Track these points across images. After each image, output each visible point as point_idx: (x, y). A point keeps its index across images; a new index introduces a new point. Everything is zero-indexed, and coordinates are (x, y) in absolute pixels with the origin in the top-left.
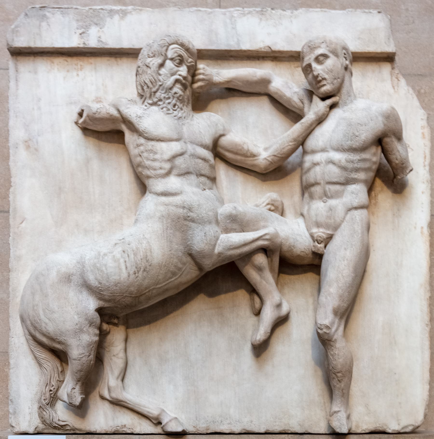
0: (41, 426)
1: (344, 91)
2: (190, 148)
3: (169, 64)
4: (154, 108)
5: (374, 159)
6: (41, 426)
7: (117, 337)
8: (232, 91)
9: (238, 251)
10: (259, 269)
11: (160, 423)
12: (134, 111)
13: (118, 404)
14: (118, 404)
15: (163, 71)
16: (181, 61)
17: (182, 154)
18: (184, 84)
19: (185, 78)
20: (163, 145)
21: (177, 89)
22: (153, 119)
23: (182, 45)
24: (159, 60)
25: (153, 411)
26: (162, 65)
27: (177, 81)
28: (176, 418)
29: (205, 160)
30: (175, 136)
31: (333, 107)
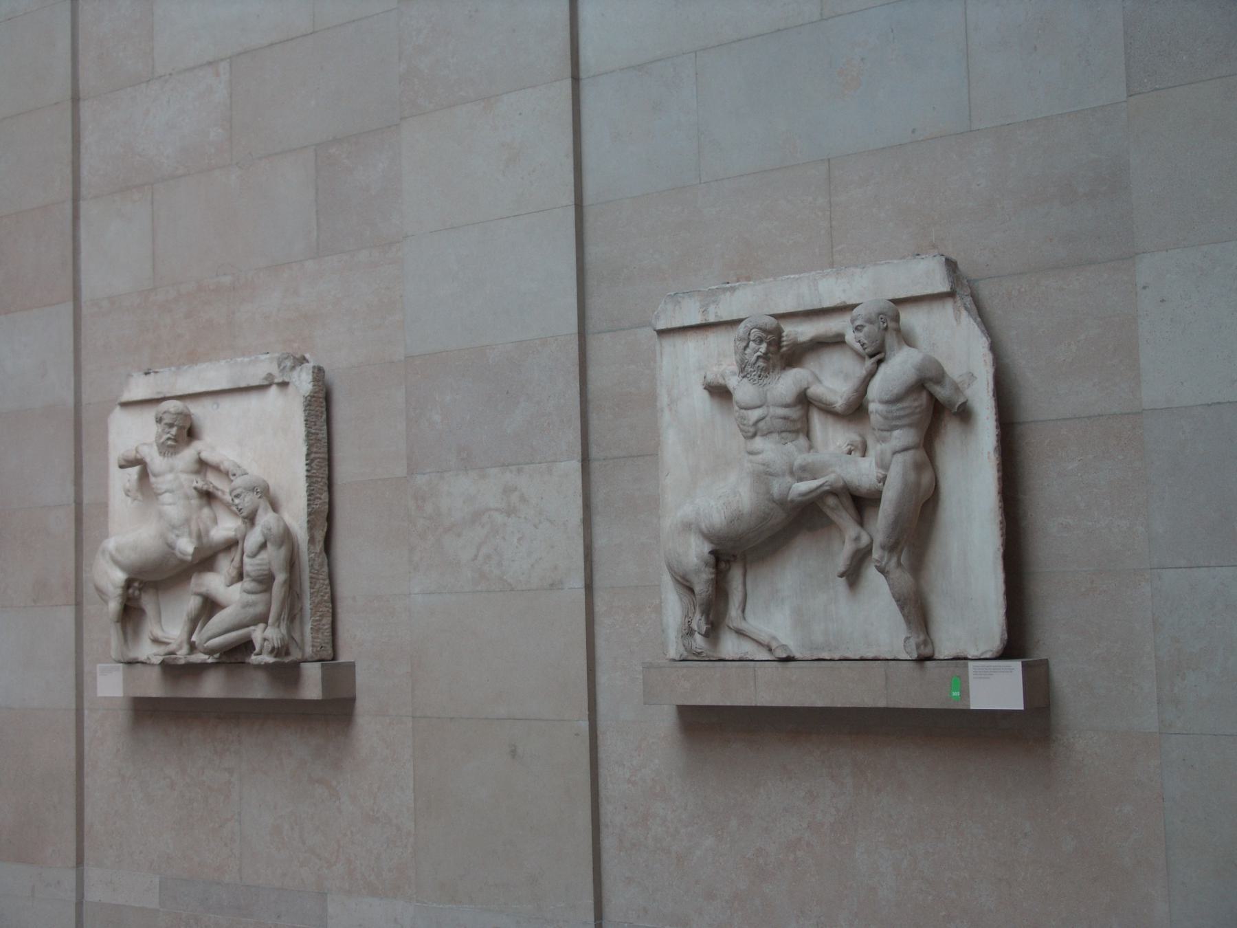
0: (685, 654)
1: (887, 348)
2: (771, 409)
3: (752, 344)
4: (745, 380)
5: (916, 404)
6: (685, 654)
7: (736, 575)
8: (820, 344)
9: (814, 494)
10: (833, 509)
11: (770, 650)
12: (733, 382)
13: (740, 633)
14: (740, 633)
15: (748, 351)
16: (761, 341)
17: (763, 418)
18: (765, 357)
19: (766, 354)
20: (750, 412)
21: (761, 363)
22: (743, 390)
23: (760, 329)
24: (744, 344)
25: (764, 638)
26: (747, 347)
27: (758, 357)
28: (784, 646)
29: (785, 418)
30: (759, 403)
31: (880, 362)
